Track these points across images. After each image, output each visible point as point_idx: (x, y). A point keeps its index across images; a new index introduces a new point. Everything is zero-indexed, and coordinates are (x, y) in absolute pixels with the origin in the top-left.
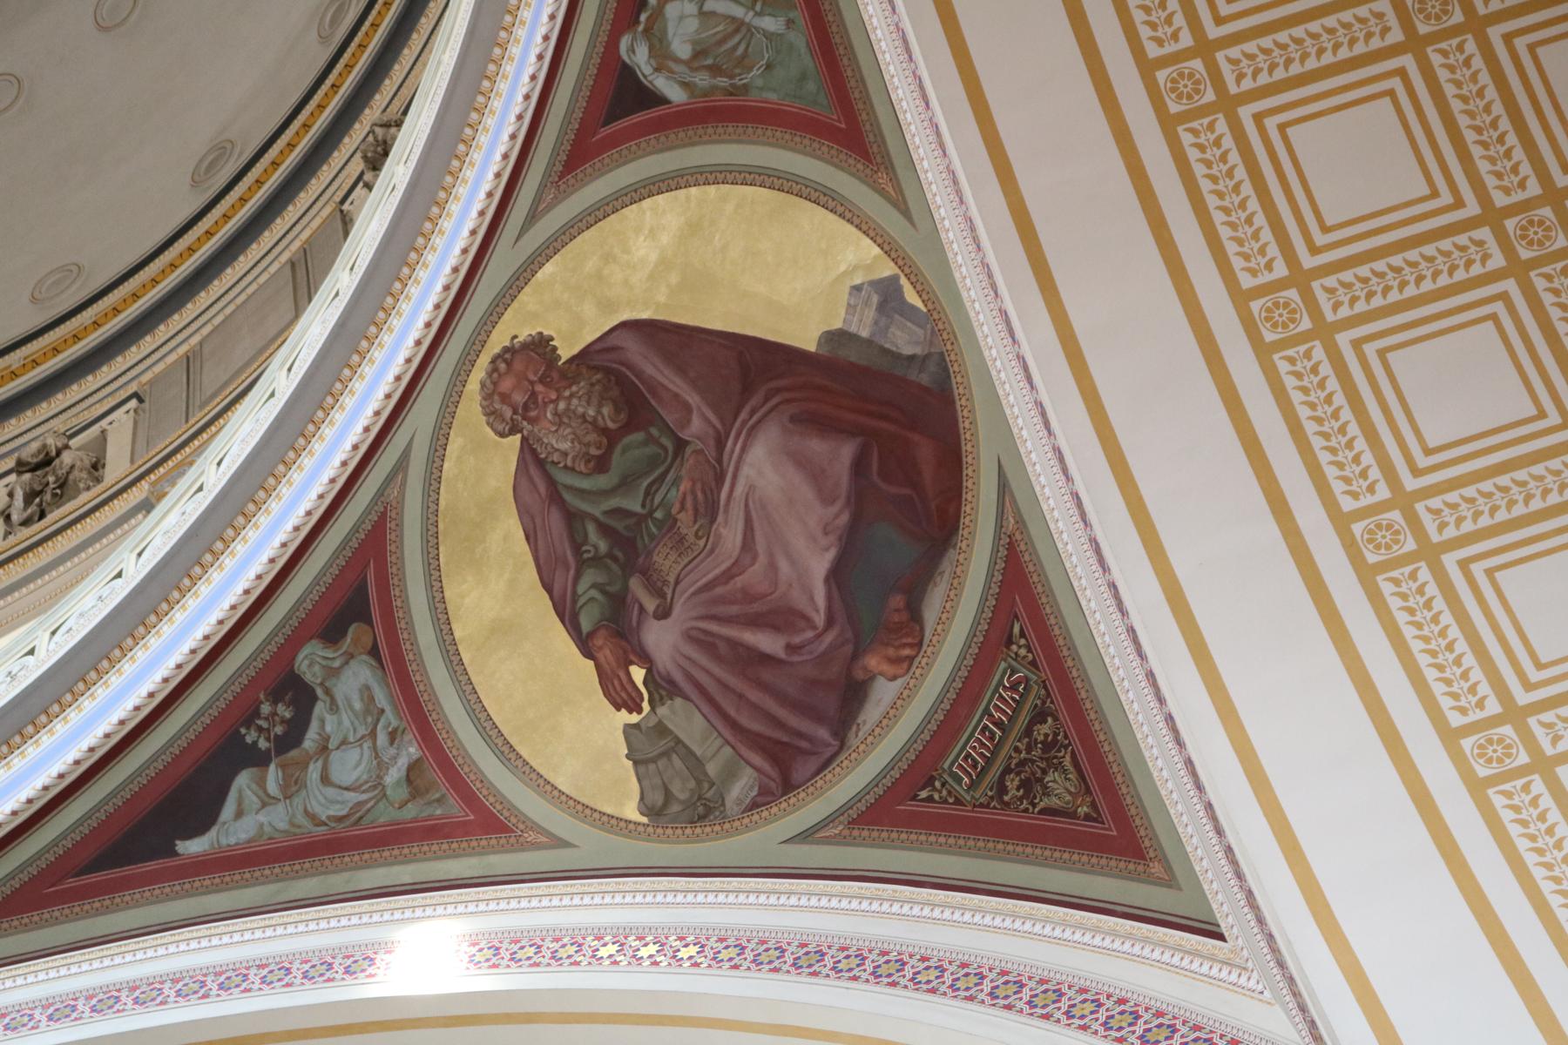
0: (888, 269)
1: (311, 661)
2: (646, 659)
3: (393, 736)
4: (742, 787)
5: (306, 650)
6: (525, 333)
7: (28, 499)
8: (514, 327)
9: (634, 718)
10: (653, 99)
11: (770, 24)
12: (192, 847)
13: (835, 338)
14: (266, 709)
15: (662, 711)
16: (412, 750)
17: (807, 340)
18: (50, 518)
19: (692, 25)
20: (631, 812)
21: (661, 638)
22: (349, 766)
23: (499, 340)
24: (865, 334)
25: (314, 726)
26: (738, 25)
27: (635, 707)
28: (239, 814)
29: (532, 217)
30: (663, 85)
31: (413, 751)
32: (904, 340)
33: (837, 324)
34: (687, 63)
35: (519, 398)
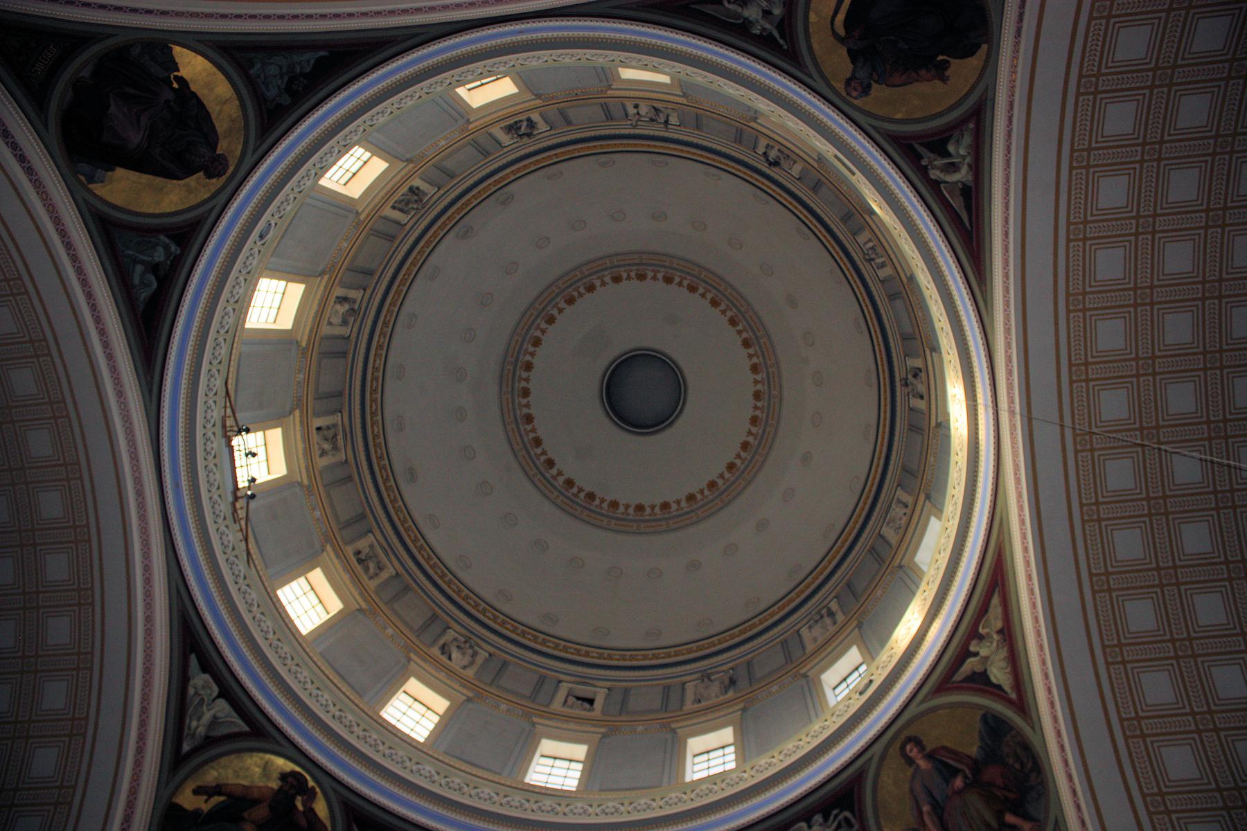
0: (91, 186)
1: (286, 100)
2: (174, 89)
3: (259, 76)
4: (136, 52)
5: (288, 103)
6: (214, 180)
7: (520, 127)
8: (216, 183)
9: (176, 73)
10: (168, 236)
11: (130, 252)
12: (322, 53)
13: (112, 170)
14: (300, 89)
15: (166, 75)
16: (252, 72)
17: (120, 172)
18: (513, 121)
19: (156, 254)
20: (177, 50)
21: (171, 96)
22: (273, 70)
23: (224, 178)
24: (99, 170)
25: (285, 81)
26: (140, 253)
27: (176, 78)
28: (308, 61)
29: (211, 210)
30: (167, 240)
31: (252, 72)
32: (86, 167)
33: (109, 173)
34: (157, 245)
35: (217, 163)
